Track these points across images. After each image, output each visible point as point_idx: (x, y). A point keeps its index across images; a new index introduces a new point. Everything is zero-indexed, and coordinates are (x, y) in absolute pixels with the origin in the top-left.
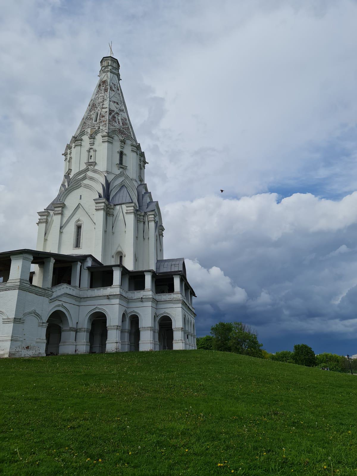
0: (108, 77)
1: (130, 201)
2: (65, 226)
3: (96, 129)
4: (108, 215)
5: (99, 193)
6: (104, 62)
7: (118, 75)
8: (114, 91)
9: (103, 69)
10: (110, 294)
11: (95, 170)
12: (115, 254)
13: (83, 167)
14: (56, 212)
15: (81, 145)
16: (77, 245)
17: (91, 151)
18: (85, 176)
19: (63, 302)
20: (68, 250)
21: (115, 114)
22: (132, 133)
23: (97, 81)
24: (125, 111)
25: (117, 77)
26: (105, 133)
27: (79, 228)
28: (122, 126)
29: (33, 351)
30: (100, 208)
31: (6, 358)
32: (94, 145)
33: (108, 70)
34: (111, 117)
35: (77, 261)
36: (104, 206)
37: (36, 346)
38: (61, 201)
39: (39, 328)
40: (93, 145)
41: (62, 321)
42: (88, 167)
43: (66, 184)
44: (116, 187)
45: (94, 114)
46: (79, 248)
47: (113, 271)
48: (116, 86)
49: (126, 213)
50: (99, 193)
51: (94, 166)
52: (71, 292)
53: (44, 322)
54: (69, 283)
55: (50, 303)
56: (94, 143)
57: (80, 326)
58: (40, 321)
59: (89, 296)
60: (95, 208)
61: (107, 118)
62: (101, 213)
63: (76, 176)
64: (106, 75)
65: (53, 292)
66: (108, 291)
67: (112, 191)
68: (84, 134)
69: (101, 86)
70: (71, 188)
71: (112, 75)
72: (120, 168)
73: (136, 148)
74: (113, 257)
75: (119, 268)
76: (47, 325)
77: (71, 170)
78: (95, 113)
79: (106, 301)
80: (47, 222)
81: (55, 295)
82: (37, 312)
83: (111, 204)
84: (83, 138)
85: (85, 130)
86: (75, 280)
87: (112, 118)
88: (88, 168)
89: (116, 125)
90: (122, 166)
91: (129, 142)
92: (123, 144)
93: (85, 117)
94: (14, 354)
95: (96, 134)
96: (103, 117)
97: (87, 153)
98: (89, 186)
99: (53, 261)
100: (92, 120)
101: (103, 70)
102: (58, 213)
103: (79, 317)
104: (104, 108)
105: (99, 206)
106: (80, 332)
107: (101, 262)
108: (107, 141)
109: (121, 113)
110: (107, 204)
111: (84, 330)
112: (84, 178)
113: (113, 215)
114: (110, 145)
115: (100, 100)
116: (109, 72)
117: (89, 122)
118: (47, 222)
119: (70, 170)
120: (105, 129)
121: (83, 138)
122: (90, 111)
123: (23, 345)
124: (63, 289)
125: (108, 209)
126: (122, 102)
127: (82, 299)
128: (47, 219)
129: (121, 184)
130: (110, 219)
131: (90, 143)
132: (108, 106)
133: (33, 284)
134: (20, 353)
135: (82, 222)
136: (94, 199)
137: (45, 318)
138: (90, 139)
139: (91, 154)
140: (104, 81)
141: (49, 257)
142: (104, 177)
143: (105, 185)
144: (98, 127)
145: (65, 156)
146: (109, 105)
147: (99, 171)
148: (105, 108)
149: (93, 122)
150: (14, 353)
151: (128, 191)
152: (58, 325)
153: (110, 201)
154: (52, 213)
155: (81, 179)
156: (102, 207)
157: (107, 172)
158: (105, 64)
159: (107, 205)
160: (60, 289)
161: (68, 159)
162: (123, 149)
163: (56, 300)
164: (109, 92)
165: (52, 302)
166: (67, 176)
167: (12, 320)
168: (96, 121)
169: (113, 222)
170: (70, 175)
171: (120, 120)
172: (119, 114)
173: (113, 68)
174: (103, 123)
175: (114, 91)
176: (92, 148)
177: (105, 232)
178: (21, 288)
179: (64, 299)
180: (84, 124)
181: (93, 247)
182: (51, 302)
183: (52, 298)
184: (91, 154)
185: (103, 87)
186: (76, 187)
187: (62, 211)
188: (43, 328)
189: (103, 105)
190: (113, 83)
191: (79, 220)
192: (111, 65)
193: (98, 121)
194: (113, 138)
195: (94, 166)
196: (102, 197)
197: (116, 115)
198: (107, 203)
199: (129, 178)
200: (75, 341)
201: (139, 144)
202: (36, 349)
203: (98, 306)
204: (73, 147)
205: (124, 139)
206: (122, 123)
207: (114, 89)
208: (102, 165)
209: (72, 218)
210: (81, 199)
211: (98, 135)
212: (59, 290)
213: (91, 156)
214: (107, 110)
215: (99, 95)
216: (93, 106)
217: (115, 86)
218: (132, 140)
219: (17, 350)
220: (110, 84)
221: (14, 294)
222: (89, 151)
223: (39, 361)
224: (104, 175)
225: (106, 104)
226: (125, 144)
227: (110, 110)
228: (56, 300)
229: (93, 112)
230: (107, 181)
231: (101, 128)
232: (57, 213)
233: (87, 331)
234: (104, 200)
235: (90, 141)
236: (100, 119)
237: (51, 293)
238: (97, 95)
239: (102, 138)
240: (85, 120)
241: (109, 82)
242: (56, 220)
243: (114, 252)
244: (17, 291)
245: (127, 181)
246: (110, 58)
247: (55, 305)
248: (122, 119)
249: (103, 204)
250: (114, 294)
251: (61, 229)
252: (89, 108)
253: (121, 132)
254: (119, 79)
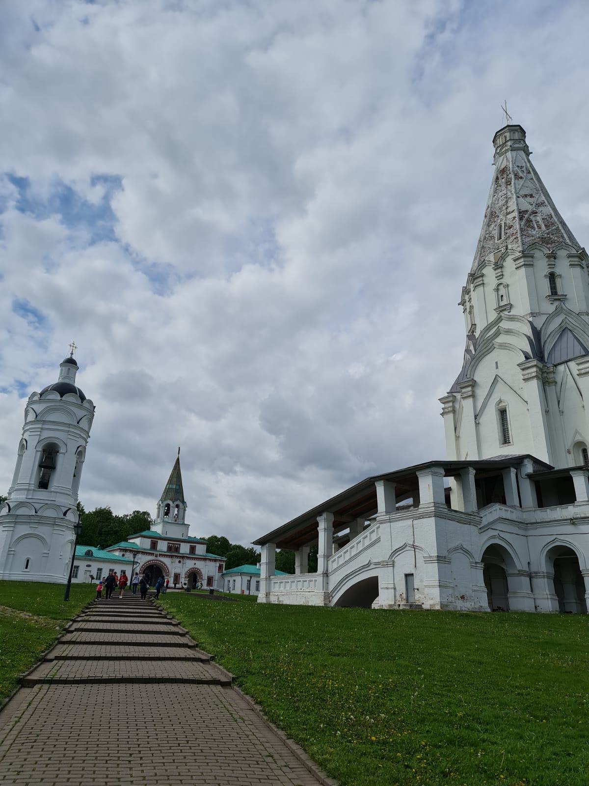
0: (509, 159)
1: (583, 353)
2: (482, 413)
3: (502, 251)
4: (547, 384)
5: (524, 353)
6: (498, 140)
7: (526, 151)
8: (521, 178)
9: (498, 151)
10: (575, 517)
11: (512, 317)
12: (572, 446)
13: (493, 316)
14: (465, 395)
15: (483, 284)
16: (506, 440)
17: (501, 287)
18: (498, 330)
19: (500, 531)
20: (493, 451)
21: (530, 215)
22: (565, 236)
23: (491, 173)
24: (546, 202)
25: (523, 152)
26: (518, 253)
27: (503, 413)
28: (544, 231)
29: (471, 603)
30: (530, 376)
31: (438, 610)
32: (504, 277)
33: (507, 148)
34: (523, 223)
35: (509, 467)
36: (537, 371)
37: (473, 595)
38: (468, 377)
39: (472, 569)
40: (502, 278)
41: (504, 560)
42: (499, 315)
43: (472, 348)
44: (552, 335)
45: (495, 228)
46: (509, 444)
47: (572, 478)
48: (524, 169)
49: (578, 375)
50: (524, 353)
51: (509, 311)
52: (508, 516)
53: (478, 561)
54: (504, 502)
55: (480, 533)
56: (502, 275)
57: (534, 569)
58: (471, 560)
59: (539, 521)
60: (522, 377)
61: (518, 227)
62: (534, 385)
63: (486, 331)
64: (505, 159)
65: (482, 517)
66: (570, 511)
67: (547, 345)
68: (485, 266)
69: (500, 178)
70: (480, 354)
71: (514, 153)
72: (553, 301)
73: (577, 259)
74: (569, 452)
75: (582, 471)
76: (483, 566)
77: (476, 324)
78: (497, 227)
79: (570, 529)
80: (454, 411)
81: (485, 522)
82: (465, 547)
83: (549, 365)
84: (484, 271)
85: (486, 259)
86: (512, 497)
87: (525, 225)
88: (501, 316)
89: (534, 232)
90: (556, 297)
91: (562, 253)
92: (553, 259)
93: (482, 238)
94: (447, 606)
95: (504, 260)
96: (510, 228)
97: (494, 294)
98: (507, 345)
99: (472, 472)
100: (493, 240)
101: (498, 153)
102: (468, 395)
103: (530, 553)
104: (509, 213)
105: (528, 374)
106: (536, 578)
107: (548, 464)
108: (524, 265)
109: (541, 209)
110: (542, 367)
111: (543, 575)
112: (497, 334)
113: (556, 383)
114: (530, 269)
115: (501, 203)
116: (510, 152)
117: (490, 244)
118: (455, 411)
119: (474, 325)
120: (516, 247)
121: (484, 271)
122: (489, 225)
123: (457, 594)
124: (495, 511)
125: (545, 375)
126: (540, 189)
127: (528, 525)
128: (454, 407)
129: (560, 328)
130: (551, 390)
131: (496, 277)
132: (516, 208)
133: (452, 508)
134: (454, 604)
135: (506, 404)
136: (518, 363)
137: (478, 557)
138: (495, 270)
139: (501, 293)
140: (504, 168)
141: (465, 468)
142: (529, 324)
143: (532, 337)
144: (505, 248)
145: (463, 305)
146: (517, 204)
147: (519, 317)
148: (512, 212)
149: (496, 241)
150: (446, 603)
151: (577, 336)
152: (500, 567)
153: (546, 361)
154: (458, 396)
155: (493, 337)
156: (534, 374)
157: (533, 314)
158: (500, 141)
159: (541, 369)
160: (491, 512)
161: (468, 310)
162: (554, 268)
163: (488, 529)
164: (515, 183)
165: (483, 532)
166: (471, 337)
167: (436, 559)
168: (501, 239)
169: (559, 395)
170: (474, 334)
171: (541, 222)
172: (536, 213)
173: (515, 141)
174: (512, 239)
175: (521, 178)
176: (501, 284)
177: (547, 412)
178: (437, 515)
179: (500, 526)
180: (482, 249)
181: (531, 441)
182: (481, 532)
183: (481, 526)
184: (501, 293)
185: (503, 180)
186: (487, 351)
187: (473, 391)
188: (477, 570)
189: (507, 208)
190: (518, 167)
191: (501, 401)
192: (513, 137)
193: (503, 238)
194: (532, 257)
195: (509, 311)
196: (531, 358)
197: (532, 217)
198: (540, 365)
199: (574, 314)
200: (532, 591)
201: (582, 249)
202: (475, 600)
203: (558, 537)
204: (472, 289)
205: (553, 251)
206: (545, 226)
207: (521, 175)
208: (522, 305)
209: (490, 398)
210: (497, 368)
211: (506, 259)
212: (489, 513)
213: (502, 296)
214: (516, 214)
215: (498, 194)
216: (491, 216)
217: (523, 170)
218: (567, 249)
219: (450, 600)
220: (513, 171)
221: (430, 524)
222: (497, 290)
223: (481, 617)
224: (528, 321)
225: (512, 205)
226: (555, 258)
227: (520, 213)
228: (488, 529)
229: (493, 226)
230: (534, 328)
231: (510, 247)
232: (466, 396)
233: (548, 577)
234: (535, 363)
235: (496, 274)
236: (507, 233)
237: (479, 518)
238: (496, 196)
239: (515, 263)
240: (483, 243)
241: (511, 166)
242: (467, 406)
243: (569, 444)
244: (432, 520)
245: (570, 320)
246: (507, 129)
247: (489, 536)
248: (543, 219)
249: (534, 369)
250: (583, 516)
251: (476, 418)
252: (485, 220)
253: (545, 241)
254: (528, 153)
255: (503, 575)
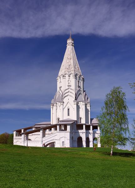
16: (69, 115)
27: (69, 109)
97: (68, 82)
112: (68, 92)
139: (69, 82)
208: (73, 87)
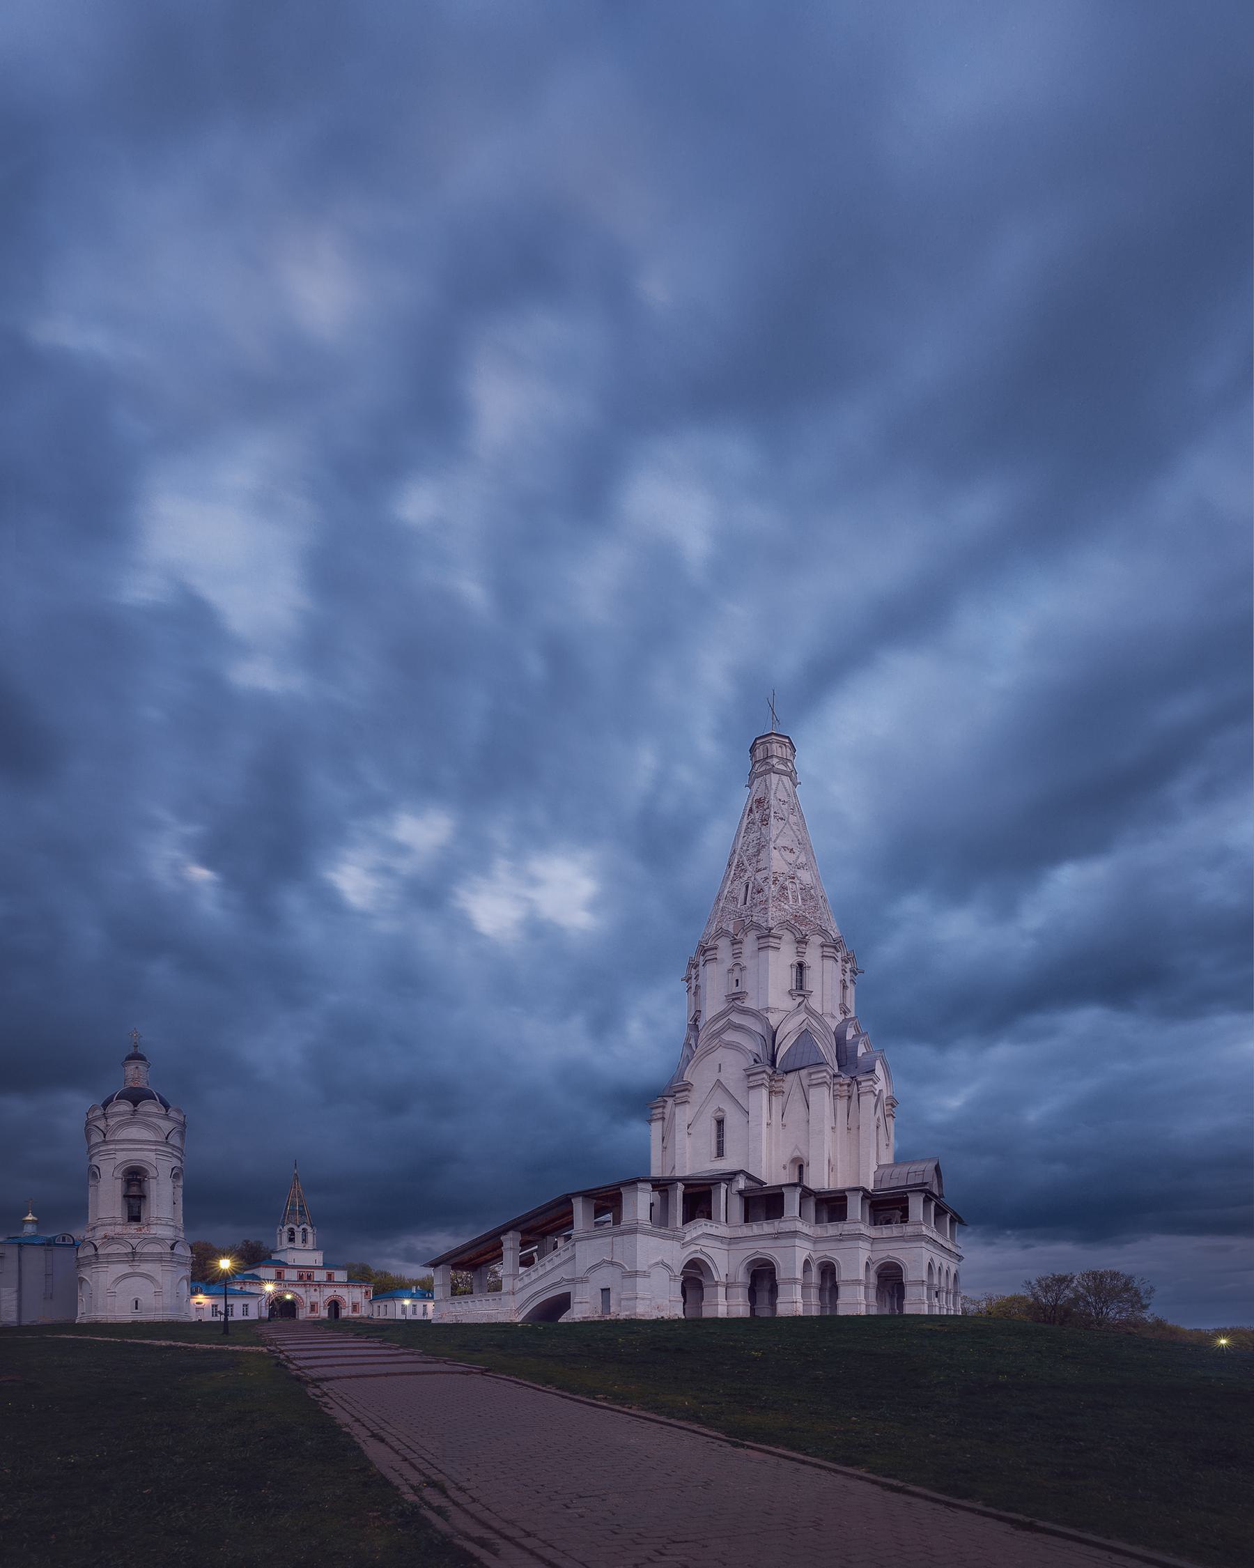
81: (688, 1239)
109: (800, 873)
124: (701, 1227)
179: (703, 1242)
255: (699, 1287)
